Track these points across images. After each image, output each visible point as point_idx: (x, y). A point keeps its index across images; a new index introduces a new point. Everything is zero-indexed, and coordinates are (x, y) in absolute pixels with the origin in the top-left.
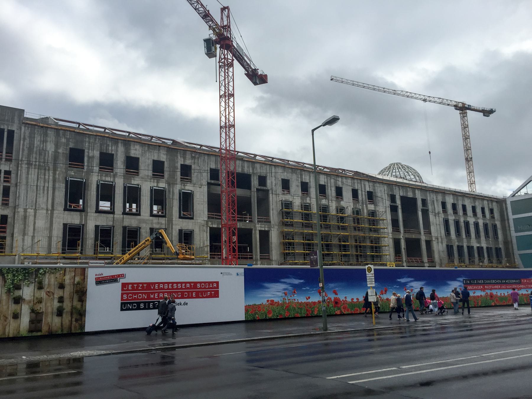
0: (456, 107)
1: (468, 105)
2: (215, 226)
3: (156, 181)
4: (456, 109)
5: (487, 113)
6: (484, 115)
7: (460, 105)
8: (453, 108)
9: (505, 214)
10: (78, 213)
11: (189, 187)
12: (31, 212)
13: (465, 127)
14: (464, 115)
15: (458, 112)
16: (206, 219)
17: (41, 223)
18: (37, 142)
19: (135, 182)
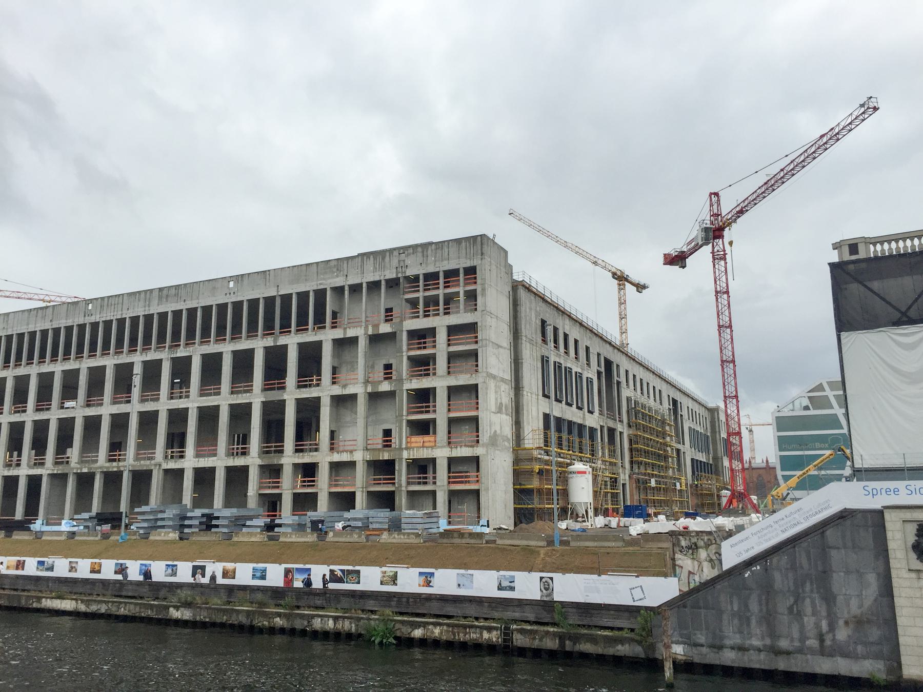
0: (614, 275)
1: (627, 275)
2: (602, 424)
3: (576, 364)
4: (613, 277)
5: (640, 287)
6: (638, 291)
7: (619, 273)
8: (610, 275)
9: (717, 425)
10: (548, 399)
11: (590, 376)
12: (529, 394)
13: (622, 302)
14: (621, 288)
15: (616, 282)
16: (598, 414)
17: (534, 409)
18: (528, 310)
19: (569, 365)
